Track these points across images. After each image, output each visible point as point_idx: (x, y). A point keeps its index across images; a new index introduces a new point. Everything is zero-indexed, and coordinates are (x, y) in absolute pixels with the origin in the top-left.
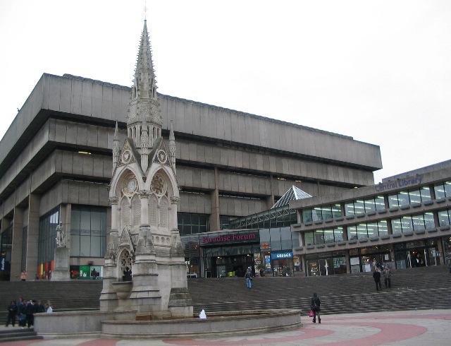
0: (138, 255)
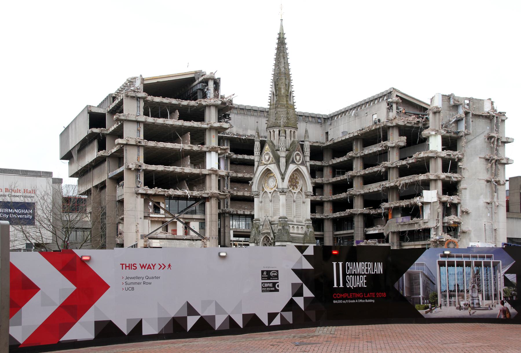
0: (278, 241)
